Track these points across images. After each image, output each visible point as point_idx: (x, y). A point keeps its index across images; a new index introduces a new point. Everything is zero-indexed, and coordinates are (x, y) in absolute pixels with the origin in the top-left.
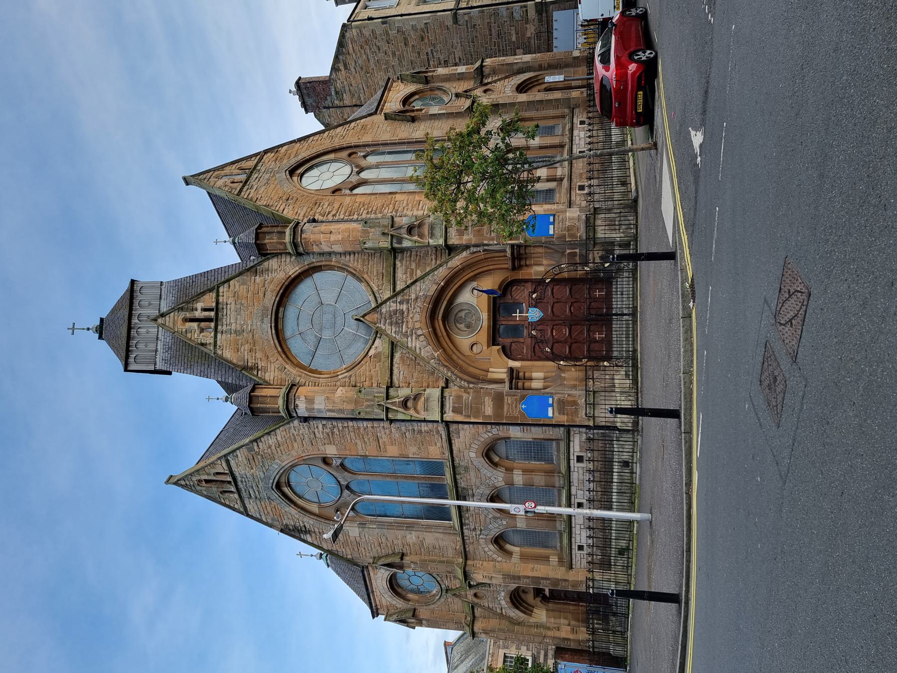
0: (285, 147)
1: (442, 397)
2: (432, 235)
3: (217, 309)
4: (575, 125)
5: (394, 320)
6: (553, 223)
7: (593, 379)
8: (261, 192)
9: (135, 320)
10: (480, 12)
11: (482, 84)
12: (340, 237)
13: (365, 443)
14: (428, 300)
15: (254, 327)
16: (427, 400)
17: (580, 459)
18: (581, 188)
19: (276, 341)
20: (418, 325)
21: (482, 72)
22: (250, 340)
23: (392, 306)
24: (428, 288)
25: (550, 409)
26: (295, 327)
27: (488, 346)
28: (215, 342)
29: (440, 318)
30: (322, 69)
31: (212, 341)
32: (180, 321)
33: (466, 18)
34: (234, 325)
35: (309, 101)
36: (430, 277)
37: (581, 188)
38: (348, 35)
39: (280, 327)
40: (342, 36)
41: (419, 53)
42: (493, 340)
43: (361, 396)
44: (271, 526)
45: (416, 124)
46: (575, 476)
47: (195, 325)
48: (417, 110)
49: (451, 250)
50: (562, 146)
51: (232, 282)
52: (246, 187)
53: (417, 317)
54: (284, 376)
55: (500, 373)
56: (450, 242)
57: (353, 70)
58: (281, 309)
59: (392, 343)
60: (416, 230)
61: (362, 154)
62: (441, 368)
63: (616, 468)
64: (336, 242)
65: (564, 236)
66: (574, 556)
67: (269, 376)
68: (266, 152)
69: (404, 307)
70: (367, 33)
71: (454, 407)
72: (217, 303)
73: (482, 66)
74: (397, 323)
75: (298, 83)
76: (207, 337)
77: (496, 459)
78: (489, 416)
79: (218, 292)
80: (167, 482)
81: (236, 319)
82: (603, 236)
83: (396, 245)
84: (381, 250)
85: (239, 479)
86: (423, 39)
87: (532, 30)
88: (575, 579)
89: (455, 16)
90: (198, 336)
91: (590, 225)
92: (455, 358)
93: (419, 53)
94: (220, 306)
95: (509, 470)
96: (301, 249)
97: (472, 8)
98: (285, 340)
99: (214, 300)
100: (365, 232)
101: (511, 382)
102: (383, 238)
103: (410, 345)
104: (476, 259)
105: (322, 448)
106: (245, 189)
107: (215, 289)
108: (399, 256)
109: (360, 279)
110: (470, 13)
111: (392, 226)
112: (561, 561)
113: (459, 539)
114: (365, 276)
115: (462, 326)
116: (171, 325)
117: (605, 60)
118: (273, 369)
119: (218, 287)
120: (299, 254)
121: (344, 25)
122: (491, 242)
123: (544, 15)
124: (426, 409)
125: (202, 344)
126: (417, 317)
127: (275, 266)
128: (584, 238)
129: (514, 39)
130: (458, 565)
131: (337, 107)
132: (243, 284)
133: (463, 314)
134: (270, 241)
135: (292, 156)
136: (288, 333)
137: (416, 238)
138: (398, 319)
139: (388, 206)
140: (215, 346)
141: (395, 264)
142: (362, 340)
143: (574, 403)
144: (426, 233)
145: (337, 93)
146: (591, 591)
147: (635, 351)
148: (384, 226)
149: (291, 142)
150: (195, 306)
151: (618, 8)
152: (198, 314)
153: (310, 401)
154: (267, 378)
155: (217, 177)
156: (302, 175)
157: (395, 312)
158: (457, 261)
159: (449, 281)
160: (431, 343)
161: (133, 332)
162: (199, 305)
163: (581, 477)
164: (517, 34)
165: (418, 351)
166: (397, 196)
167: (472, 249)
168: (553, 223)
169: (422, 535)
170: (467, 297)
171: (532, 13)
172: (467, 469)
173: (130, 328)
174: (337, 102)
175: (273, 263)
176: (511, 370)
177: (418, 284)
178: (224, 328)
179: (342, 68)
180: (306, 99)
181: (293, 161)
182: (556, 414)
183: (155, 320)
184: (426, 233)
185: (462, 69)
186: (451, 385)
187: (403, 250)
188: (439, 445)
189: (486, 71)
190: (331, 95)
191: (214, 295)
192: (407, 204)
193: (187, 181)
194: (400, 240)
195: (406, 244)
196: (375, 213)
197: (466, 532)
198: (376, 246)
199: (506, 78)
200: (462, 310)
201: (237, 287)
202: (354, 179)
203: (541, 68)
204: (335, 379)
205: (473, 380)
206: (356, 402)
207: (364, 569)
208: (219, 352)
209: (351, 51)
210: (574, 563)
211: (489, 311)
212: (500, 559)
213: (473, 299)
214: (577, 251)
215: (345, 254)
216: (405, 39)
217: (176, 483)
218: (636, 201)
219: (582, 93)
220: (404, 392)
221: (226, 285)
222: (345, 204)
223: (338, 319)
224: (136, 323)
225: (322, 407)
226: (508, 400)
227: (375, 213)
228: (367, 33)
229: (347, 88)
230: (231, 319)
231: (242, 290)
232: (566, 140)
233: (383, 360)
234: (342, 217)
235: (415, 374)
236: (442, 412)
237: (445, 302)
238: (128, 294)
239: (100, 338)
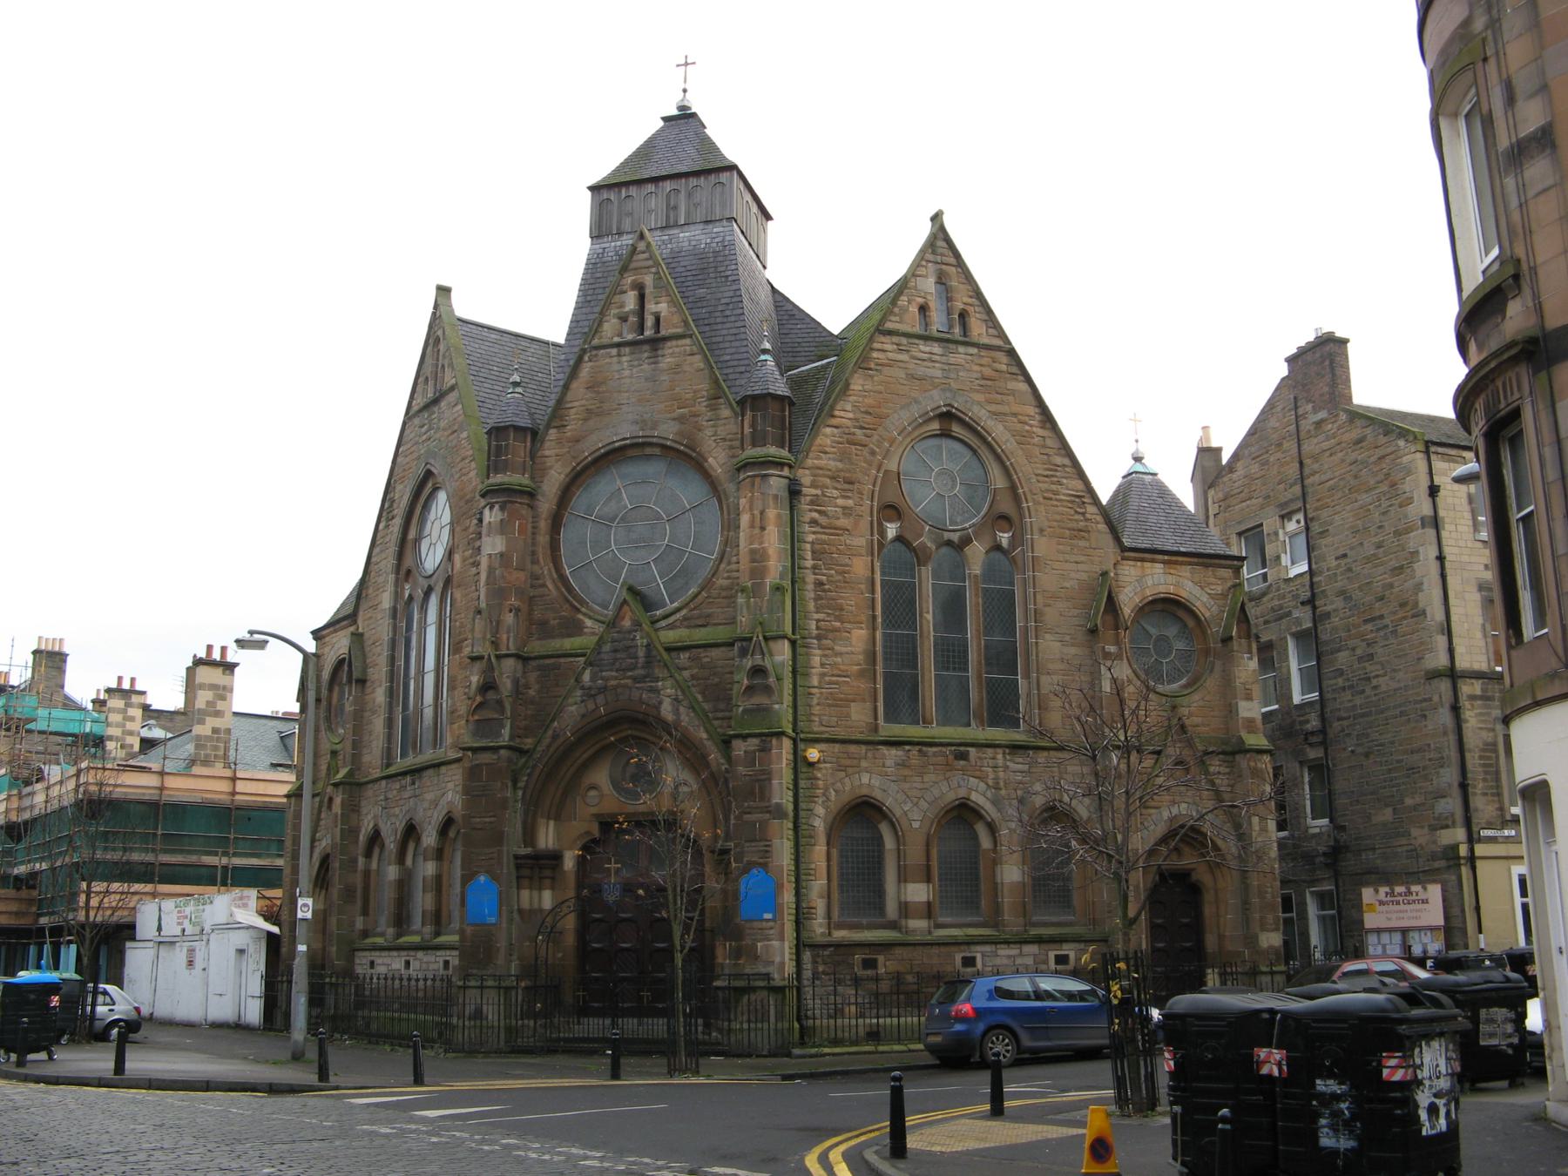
0: (1024, 387)
52: (904, 341)
56: (736, 743)
61: (1005, 543)
106: (895, 339)
135: (993, 408)
139: (838, 618)
156: (945, 434)
174: (1306, 425)
181: (980, 413)
190: (1315, 410)
193: (937, 218)
222: (845, 538)
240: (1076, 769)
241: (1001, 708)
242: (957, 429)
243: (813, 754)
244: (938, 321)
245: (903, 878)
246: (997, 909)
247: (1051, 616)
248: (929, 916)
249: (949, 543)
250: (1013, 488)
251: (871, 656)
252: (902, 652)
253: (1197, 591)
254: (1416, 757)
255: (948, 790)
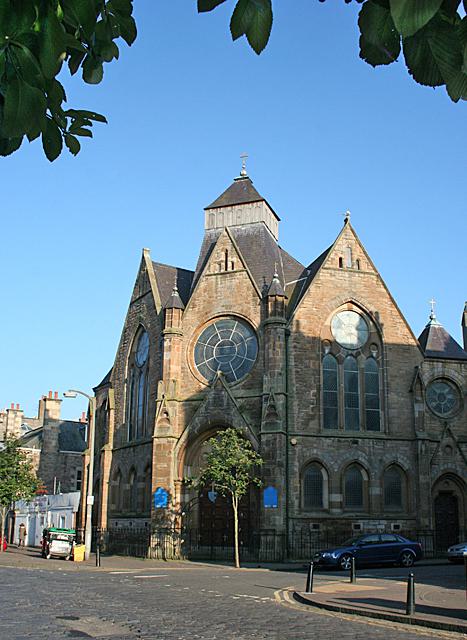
52: (333, 272)
61: (374, 355)
157: (222, 401)
161: (229, 208)
240: (405, 447)
241: (372, 423)
242: (355, 308)
243: (294, 441)
244: (347, 263)
245: (330, 492)
246: (370, 505)
247: (393, 385)
248: (341, 507)
249: (352, 355)
251: (318, 400)
252: (331, 399)
253: (456, 375)
255: (349, 456)
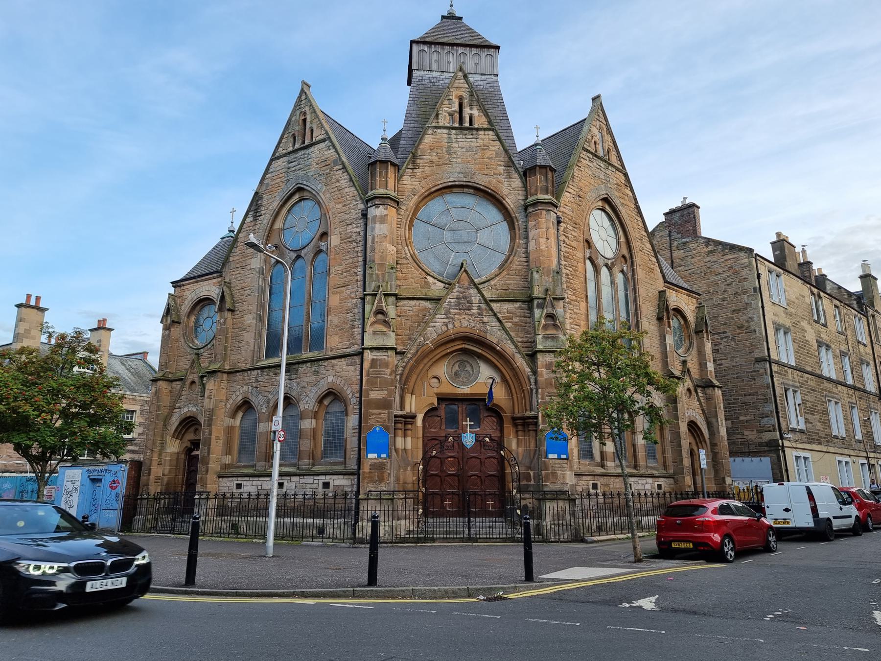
0: (630, 194)
1: (387, 349)
2: (546, 338)
3: (471, 129)
4: (657, 479)
5: (462, 301)
6: (559, 458)
7: (405, 498)
8: (587, 170)
9: (460, 50)
10: (768, 384)
11: (696, 387)
12: (543, 248)
13: (342, 274)
14: (482, 334)
15: (454, 165)
16: (384, 333)
17: (326, 485)
18: (595, 486)
19: (441, 186)
20: (457, 324)
21: (708, 387)
22: (441, 162)
23: (476, 299)
24: (494, 334)
25: (375, 456)
26: (454, 205)
27: (437, 394)
28: (440, 128)
29: (464, 346)
30: (708, 229)
31: (441, 124)
32: (460, 93)
33: (762, 371)
34: (456, 145)
35: (676, 217)
36: (505, 336)
37: (595, 486)
38: (742, 254)
39: (455, 190)
40: (741, 249)
41: (725, 324)
42: (443, 399)
43: (388, 270)
44: (261, 182)
45: (656, 322)
46: (309, 480)
47: (456, 108)
48: (669, 323)
49: (532, 356)
50: (636, 467)
51: (498, 143)
52: (591, 156)
53: (465, 323)
54: (407, 194)
55: (412, 405)
56: (539, 356)
57: (708, 259)
58: (472, 191)
59: (439, 299)
60: (550, 322)
62: (415, 348)
63: (317, 521)
64: (538, 244)
65: (547, 469)
66: (231, 479)
67: (407, 180)
68: (626, 175)
69: (475, 311)
70: (745, 272)
71: (377, 360)
72: (478, 129)
73: (714, 386)
74: (459, 303)
75: (693, 205)
76: (445, 120)
77: (326, 402)
78: (368, 394)
79: (489, 130)
80: (304, 83)
81: (462, 148)
82: (547, 508)
83: (536, 302)
84: (531, 288)
85: (307, 151)
86: (740, 328)
87: (750, 437)
88: (208, 481)
89: (763, 360)
90: (446, 111)
91: (558, 495)
92: (425, 361)
93: (725, 324)
94: (474, 132)
95: (315, 415)
96: (530, 210)
97: (772, 377)
98: (442, 195)
99: (481, 126)
100: (548, 272)
101: (401, 416)
102: (542, 290)
103: (437, 316)
104: (522, 380)
105: (337, 231)
106: (589, 155)
107: (491, 127)
108: (525, 306)
109: (502, 267)
110: (766, 374)
111: (554, 299)
112: (226, 466)
113: (248, 366)
114: (505, 272)
115: (456, 368)
116: (456, 85)
117: (723, 510)
118: (414, 183)
119: (493, 130)
120: (526, 208)
121: (751, 250)
122: (540, 396)
123: (766, 449)
124: (374, 333)
125: (437, 115)
126: (465, 323)
127: (514, 185)
128: (545, 489)
129: (742, 418)
130: (223, 365)
131: (671, 244)
132: (497, 154)
133: (468, 368)
134: (538, 180)
135: (622, 201)
136: (449, 198)
137: (543, 322)
138: (464, 304)
139: (574, 294)
140: (436, 127)
141: (517, 301)
142: (442, 270)
143: (381, 480)
144: (548, 332)
145: (685, 243)
146: (197, 497)
147: (433, 540)
148: (554, 292)
149: (636, 200)
150: (475, 108)
151: (775, 523)
152: (467, 111)
153: (383, 219)
154: (404, 178)
155: (600, 129)
156: (603, 210)
157: (470, 302)
158: (521, 362)
159: (501, 355)
160: (440, 337)
161: (449, 48)
162: (475, 112)
163: (309, 486)
164: (747, 421)
165: (432, 324)
166: (584, 303)
167: (533, 377)
168: (559, 458)
169: (252, 329)
170: (485, 373)
171: (767, 436)
172: (316, 373)
173: (453, 45)
174: (675, 244)
175: (517, 183)
176: (413, 417)
177: (498, 324)
178: (454, 136)
179: (710, 248)
180: (678, 214)
181: (617, 202)
182: (371, 461)
183: (461, 70)
184: (548, 332)
185: (711, 366)
186: (399, 357)
187: (531, 309)
188: (340, 345)
189: (709, 391)
190: (682, 238)
191: (486, 126)
192: (576, 313)
194: (541, 307)
195: (537, 312)
196: (567, 282)
197: (255, 373)
198: (535, 283)
199: (703, 411)
200: (472, 367)
201: (493, 148)
202: (600, 261)
203: (713, 445)
204: (404, 244)
205: (404, 379)
206: (382, 265)
207: (219, 273)
208: (430, 132)
209: (727, 257)
210: (224, 479)
211: (472, 394)
212: (228, 406)
213: (483, 379)
214: (532, 483)
215: (527, 252)
216: (739, 310)
217: (302, 91)
218: (583, 541)
219: (690, 486)
220: (392, 311)
221: (495, 137)
223: (463, 246)
224: (457, 51)
225: (377, 231)
226: (384, 414)
227: (567, 282)
228: (745, 272)
229: (690, 253)
230: (462, 143)
231: (491, 153)
232: (642, 471)
233: (424, 290)
234: (563, 249)
235: (409, 322)
236: (372, 349)
237: (480, 351)
238: (486, 44)
239: (443, 17)
250: (628, 242)
254: (748, 397)
